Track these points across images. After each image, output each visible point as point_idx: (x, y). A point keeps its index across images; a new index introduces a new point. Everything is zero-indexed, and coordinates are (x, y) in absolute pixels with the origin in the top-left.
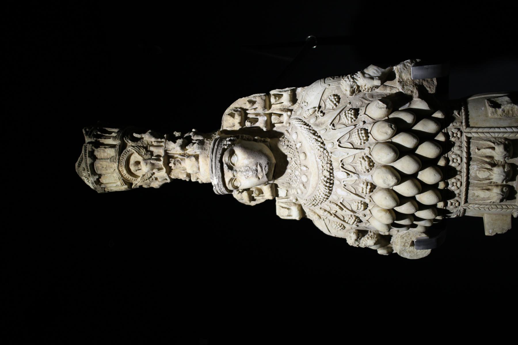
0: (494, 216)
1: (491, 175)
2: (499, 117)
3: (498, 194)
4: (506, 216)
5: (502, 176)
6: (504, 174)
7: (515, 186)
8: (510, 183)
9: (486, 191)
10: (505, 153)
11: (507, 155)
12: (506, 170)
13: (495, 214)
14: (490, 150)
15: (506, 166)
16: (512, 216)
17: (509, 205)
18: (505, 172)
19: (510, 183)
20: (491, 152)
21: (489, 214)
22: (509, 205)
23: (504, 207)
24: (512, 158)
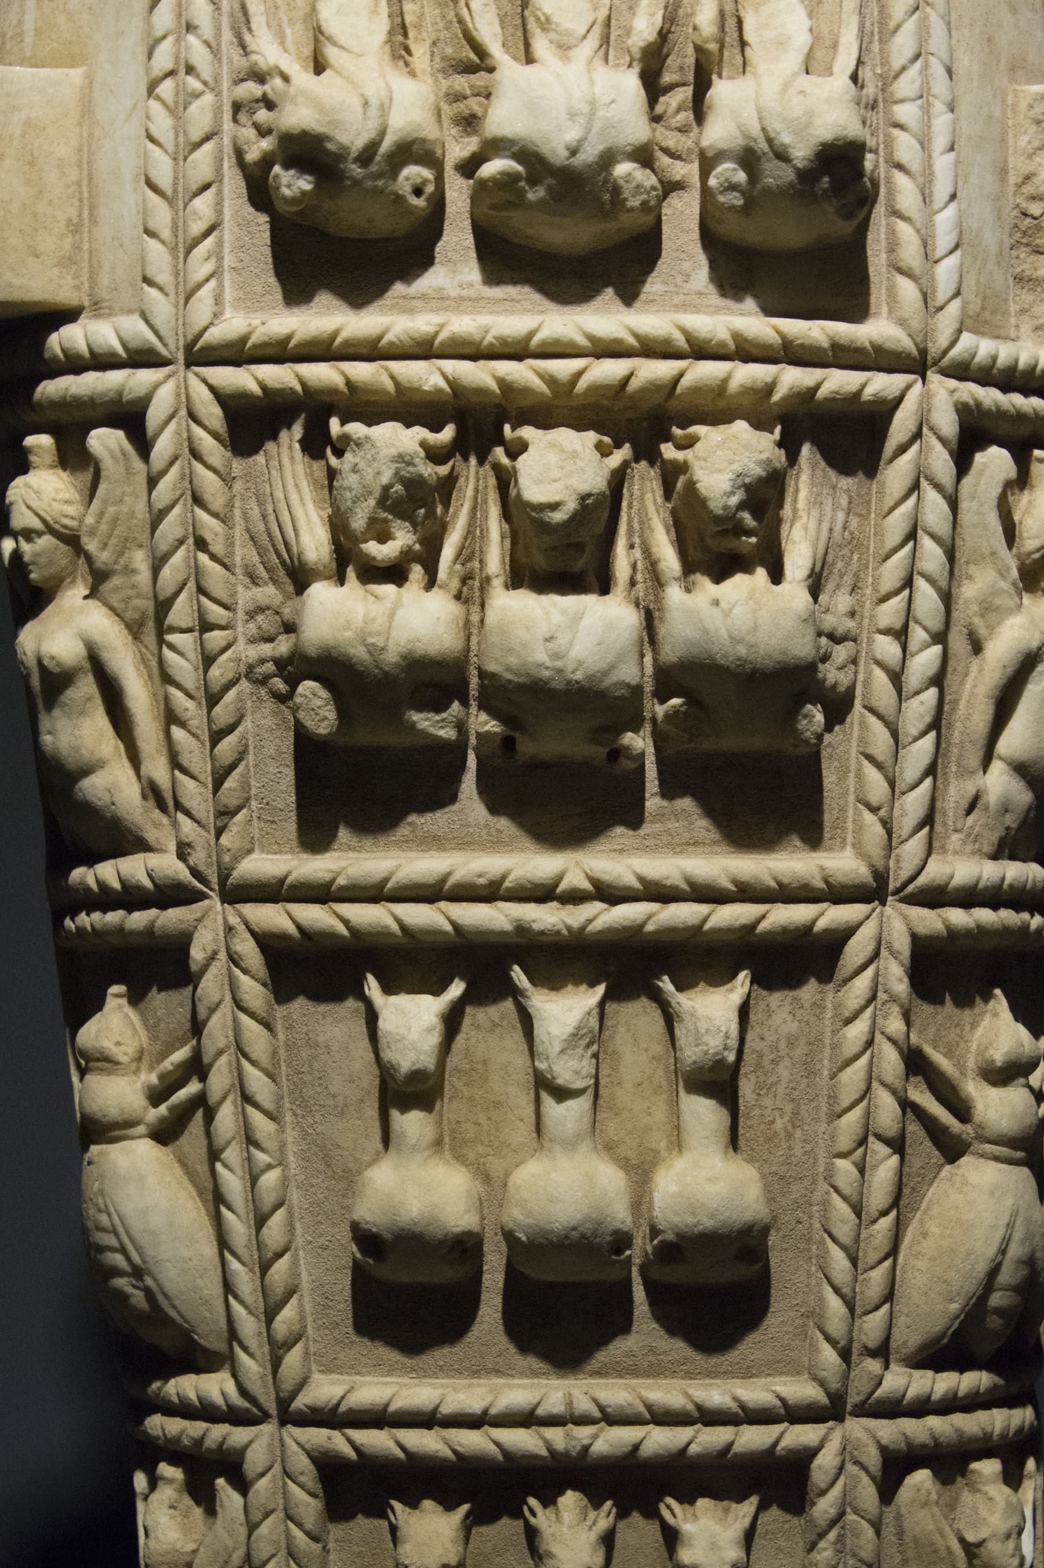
0: (64, 150)
1: (564, 48)
2: (1018, 165)
3: (384, 110)
4: (68, 262)
5: (572, 135)
6: (589, 155)
7: (430, 280)
8: (457, 238)
9: (382, 25)
10: (801, 153)
11: (776, 175)
12: (623, 169)
13: (86, 158)
14: (802, 40)
15: (647, 179)
16: (68, 315)
17: (217, 254)
18: (608, 159)
19: (457, 238)
20: (782, 43)
21: (87, 107)
22: (217, 254)
23: (203, 204)
24: (709, 238)
